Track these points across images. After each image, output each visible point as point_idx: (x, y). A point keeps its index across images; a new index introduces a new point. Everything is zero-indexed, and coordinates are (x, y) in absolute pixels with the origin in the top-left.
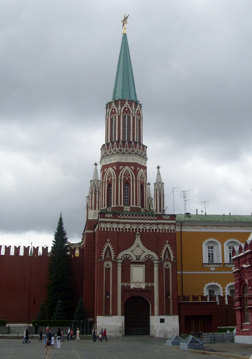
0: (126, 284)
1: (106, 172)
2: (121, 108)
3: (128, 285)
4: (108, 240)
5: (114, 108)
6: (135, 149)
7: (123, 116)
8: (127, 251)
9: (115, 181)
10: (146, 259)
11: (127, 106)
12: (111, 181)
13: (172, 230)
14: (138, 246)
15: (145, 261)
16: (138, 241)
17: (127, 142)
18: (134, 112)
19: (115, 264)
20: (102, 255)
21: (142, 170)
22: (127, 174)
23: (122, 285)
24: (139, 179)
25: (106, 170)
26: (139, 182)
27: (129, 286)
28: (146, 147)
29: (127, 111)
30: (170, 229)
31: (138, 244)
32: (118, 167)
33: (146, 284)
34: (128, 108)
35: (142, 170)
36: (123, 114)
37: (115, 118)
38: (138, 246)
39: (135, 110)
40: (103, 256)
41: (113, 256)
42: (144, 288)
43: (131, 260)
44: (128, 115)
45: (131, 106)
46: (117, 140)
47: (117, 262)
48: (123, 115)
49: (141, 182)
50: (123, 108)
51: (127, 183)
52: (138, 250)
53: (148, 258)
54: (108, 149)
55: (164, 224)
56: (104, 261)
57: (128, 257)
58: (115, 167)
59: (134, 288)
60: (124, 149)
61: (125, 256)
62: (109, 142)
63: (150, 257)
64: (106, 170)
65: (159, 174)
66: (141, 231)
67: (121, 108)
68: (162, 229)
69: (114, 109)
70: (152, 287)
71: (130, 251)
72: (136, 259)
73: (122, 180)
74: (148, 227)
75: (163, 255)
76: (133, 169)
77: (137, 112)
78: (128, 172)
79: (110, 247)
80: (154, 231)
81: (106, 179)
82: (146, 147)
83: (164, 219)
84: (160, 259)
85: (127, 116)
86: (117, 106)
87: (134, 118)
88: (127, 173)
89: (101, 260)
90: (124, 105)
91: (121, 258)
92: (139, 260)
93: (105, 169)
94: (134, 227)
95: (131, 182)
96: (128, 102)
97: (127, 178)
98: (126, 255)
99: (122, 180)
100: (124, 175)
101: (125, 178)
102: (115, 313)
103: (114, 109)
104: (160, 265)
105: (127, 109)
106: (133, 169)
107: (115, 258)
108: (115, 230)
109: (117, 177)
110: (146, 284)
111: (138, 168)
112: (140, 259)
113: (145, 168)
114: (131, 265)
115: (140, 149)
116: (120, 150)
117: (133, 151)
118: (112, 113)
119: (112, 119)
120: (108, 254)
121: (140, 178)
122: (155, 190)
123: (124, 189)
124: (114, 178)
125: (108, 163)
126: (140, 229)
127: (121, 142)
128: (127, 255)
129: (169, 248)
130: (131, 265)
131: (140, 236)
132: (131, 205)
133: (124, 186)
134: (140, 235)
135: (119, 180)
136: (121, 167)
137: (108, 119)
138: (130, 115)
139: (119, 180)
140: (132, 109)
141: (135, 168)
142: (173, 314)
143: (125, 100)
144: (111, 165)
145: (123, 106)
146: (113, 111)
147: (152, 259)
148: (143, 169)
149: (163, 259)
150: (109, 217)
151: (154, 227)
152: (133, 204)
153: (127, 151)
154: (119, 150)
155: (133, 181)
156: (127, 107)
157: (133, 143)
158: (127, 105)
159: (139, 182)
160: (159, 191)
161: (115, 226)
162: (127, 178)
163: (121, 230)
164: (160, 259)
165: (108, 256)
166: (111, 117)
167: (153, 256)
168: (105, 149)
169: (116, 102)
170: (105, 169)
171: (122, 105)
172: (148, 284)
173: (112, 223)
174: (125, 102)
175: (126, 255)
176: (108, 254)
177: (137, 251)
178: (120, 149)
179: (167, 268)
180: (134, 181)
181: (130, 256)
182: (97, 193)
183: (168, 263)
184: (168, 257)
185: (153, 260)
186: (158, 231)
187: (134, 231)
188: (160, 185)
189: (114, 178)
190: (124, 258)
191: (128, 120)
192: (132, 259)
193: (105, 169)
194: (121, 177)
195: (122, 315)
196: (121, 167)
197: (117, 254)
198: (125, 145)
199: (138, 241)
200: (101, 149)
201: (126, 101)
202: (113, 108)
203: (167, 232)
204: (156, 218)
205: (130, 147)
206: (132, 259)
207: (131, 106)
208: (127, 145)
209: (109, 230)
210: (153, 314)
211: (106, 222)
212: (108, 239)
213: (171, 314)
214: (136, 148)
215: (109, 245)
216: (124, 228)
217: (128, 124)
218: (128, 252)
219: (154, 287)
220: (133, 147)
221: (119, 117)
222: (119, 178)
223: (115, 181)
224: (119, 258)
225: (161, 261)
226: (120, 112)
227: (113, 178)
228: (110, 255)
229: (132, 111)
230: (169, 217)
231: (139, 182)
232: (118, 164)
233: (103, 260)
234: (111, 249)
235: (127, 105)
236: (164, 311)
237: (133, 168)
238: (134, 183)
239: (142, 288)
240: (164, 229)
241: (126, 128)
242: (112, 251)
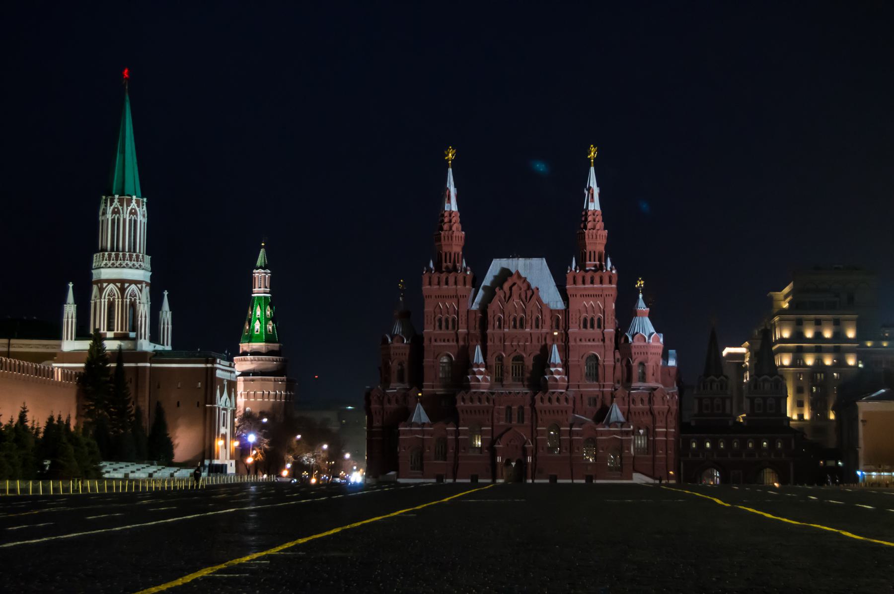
22: (133, 295)
32: (123, 285)
37: (118, 220)
45: (138, 206)
50: (129, 208)
58: (119, 285)
86: (122, 205)
93: (105, 285)
109: (122, 298)
118: (114, 212)
119: (113, 220)
136: (126, 285)
153: (134, 265)
171: (128, 205)
221: (124, 220)
232: (123, 282)
237: (139, 286)
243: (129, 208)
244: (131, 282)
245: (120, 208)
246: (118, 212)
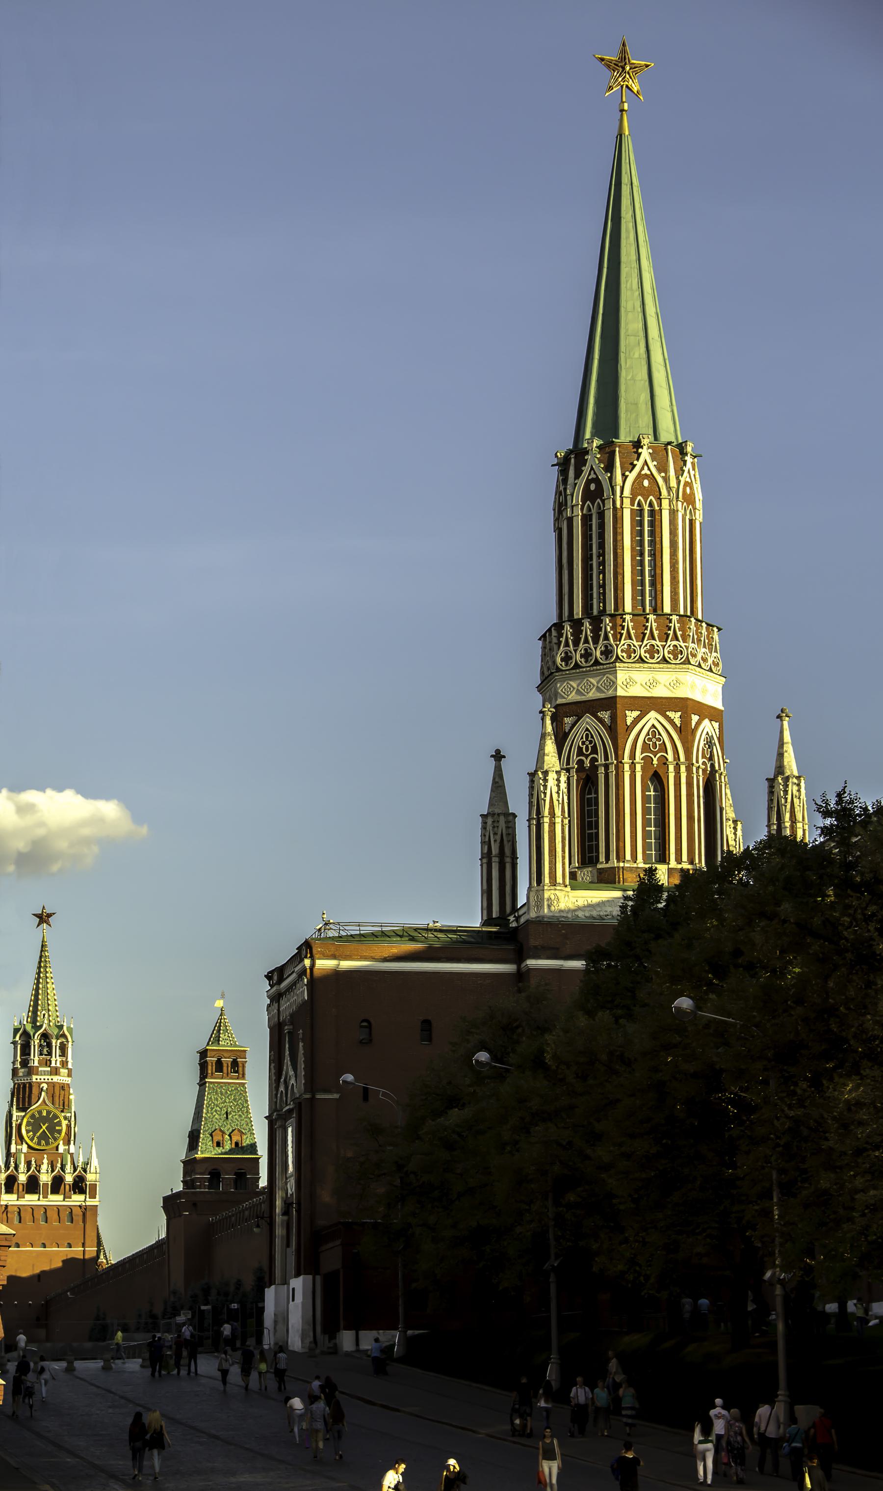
2: (625, 478)
5: (593, 476)
6: (683, 645)
9: (612, 768)
11: (646, 467)
12: (594, 768)
17: (652, 617)
24: (699, 761)
26: (697, 772)
29: (646, 489)
34: (652, 477)
37: (601, 515)
39: (679, 483)
44: (651, 505)
45: (663, 468)
46: (611, 608)
49: (704, 771)
50: (632, 476)
54: (576, 643)
62: (578, 612)
67: (625, 478)
69: (593, 480)
76: (678, 722)
77: (684, 490)
78: (660, 734)
81: (575, 758)
85: (646, 508)
87: (673, 513)
88: (654, 740)
90: (635, 462)
96: (650, 451)
99: (638, 767)
100: (645, 748)
101: (647, 761)
103: (597, 481)
105: (646, 483)
106: (678, 722)
111: (695, 718)
117: (676, 652)
121: (703, 758)
123: (646, 799)
124: (606, 758)
127: (628, 617)
132: (673, 864)
133: (645, 789)
135: (627, 767)
137: (570, 520)
139: (627, 767)
140: (666, 480)
141: (685, 719)
143: (637, 444)
146: (593, 487)
148: (711, 720)
152: (679, 860)
153: (652, 651)
154: (622, 651)
156: (649, 473)
158: (646, 463)
159: (701, 771)
162: (655, 762)
168: (563, 640)
170: (566, 720)
174: (640, 450)
180: (683, 768)
189: (606, 758)
196: (631, 715)
198: (646, 629)
200: (544, 636)
201: (642, 447)
205: (665, 638)
207: (663, 468)
208: (654, 628)
222: (626, 759)
226: (622, 493)
229: (669, 489)
231: (701, 771)
235: (646, 463)
237: (676, 716)
243: (632, 476)
244: (645, 704)
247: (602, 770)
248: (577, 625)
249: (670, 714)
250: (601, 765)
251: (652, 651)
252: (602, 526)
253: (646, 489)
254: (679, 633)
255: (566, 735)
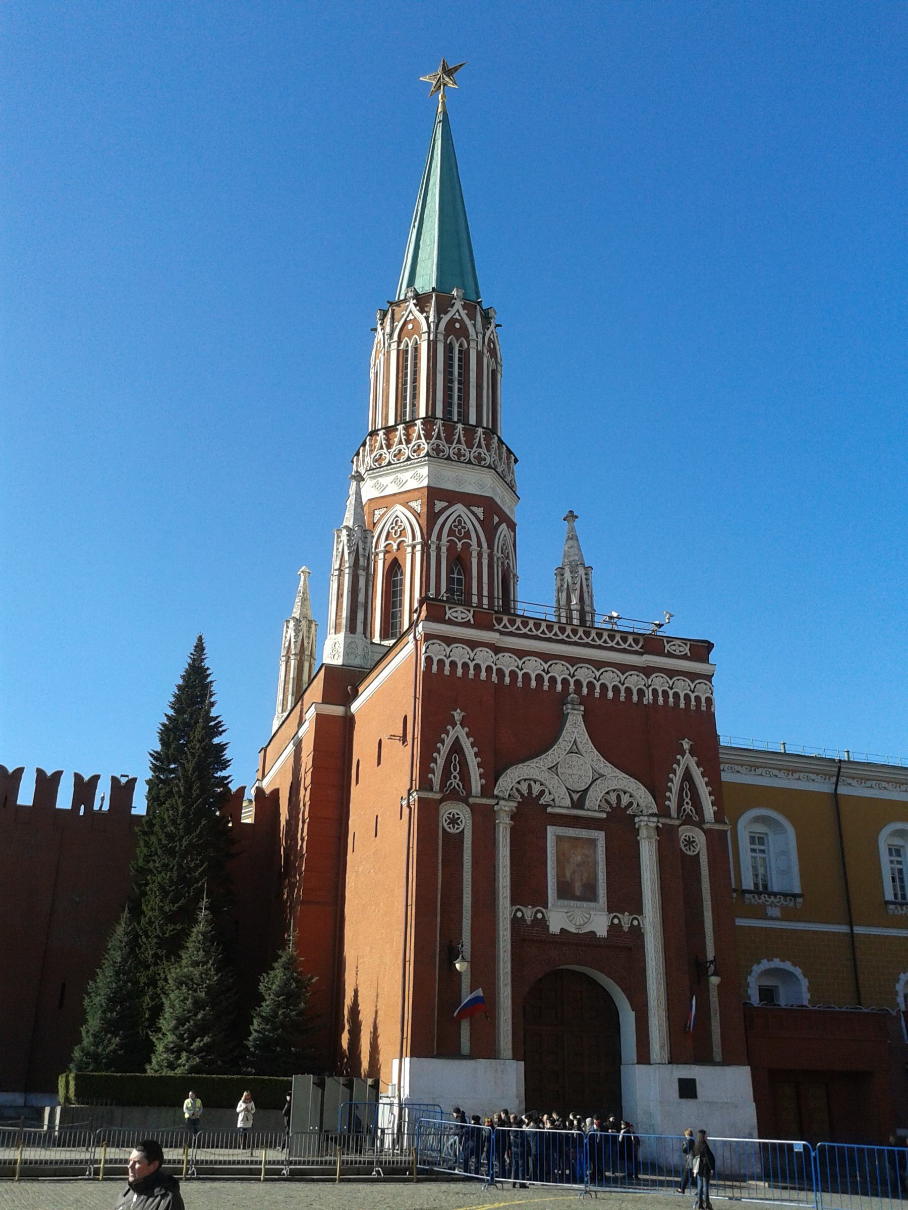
0: (528, 913)
1: (379, 520)
3: (539, 916)
4: (458, 715)
5: (411, 317)
7: (445, 343)
8: (532, 765)
10: (609, 810)
13: (703, 700)
14: (575, 750)
15: (604, 815)
16: (575, 728)
18: (480, 336)
19: (484, 819)
20: (430, 776)
21: (504, 526)
22: (458, 530)
23: (515, 914)
25: (382, 516)
27: (542, 924)
28: (516, 461)
30: (693, 696)
31: (575, 741)
32: (430, 505)
33: (612, 915)
34: (461, 321)
35: (504, 526)
36: (446, 337)
37: (416, 349)
38: (575, 750)
40: (436, 779)
41: (476, 784)
42: (602, 931)
43: (550, 805)
47: (496, 808)
48: (446, 339)
49: (503, 563)
50: (445, 319)
51: (459, 561)
52: (573, 768)
53: (614, 802)
55: (671, 673)
56: (441, 801)
57: (535, 792)
58: (417, 505)
59: (562, 929)
60: (449, 448)
61: (524, 788)
63: (625, 800)
64: (382, 516)
65: (573, 537)
66: (585, 691)
67: (440, 319)
68: (665, 693)
70: (637, 933)
71: (545, 769)
72: (568, 802)
73: (444, 549)
74: (610, 678)
75: (673, 796)
79: (466, 743)
80: (635, 698)
81: (382, 544)
82: (516, 461)
83: (670, 655)
84: (663, 812)
87: (480, 355)
88: (460, 527)
89: (430, 795)
91: (509, 795)
92: (583, 809)
94: (559, 671)
95: (473, 559)
97: (459, 545)
98: (529, 784)
99: (444, 549)
100: (451, 532)
102: (485, 1049)
104: (666, 838)
105: (457, 325)
107: (487, 791)
108: (483, 675)
110: (613, 918)
112: (587, 804)
113: (512, 526)
114: (550, 830)
115: (500, 458)
116: (437, 450)
117: (480, 458)
119: (402, 355)
120: (455, 774)
122: (559, 590)
123: (450, 580)
124: (414, 538)
125: (392, 489)
126: (578, 683)
128: (532, 783)
129: (696, 772)
130: (550, 830)
131: (582, 708)
133: (450, 571)
134: (581, 704)
135: (433, 547)
137: (389, 352)
138: (469, 345)
140: (474, 325)
142: (728, 1061)
144: (403, 498)
145: (446, 313)
147: (629, 812)
149: (674, 813)
150: (459, 620)
151: (635, 681)
153: (459, 454)
155: (480, 555)
157: (480, 431)
158: (458, 311)
160: (578, 592)
161: (484, 657)
162: (459, 545)
163: (507, 680)
164: (663, 812)
165: (455, 782)
166: (398, 346)
167: (638, 797)
169: (421, 301)
172: (619, 915)
173: (473, 645)
175: (530, 786)
176: (455, 774)
177: (571, 772)
178: (438, 445)
179: (690, 853)
180: (485, 556)
181: (543, 788)
182: (361, 572)
183: (690, 834)
184: (690, 807)
185: (635, 816)
186: (651, 697)
187: (559, 687)
188: (581, 571)
189: (414, 538)
190: (522, 795)
191: (460, 360)
192: (552, 803)
193: (377, 512)
194: (439, 538)
195: (515, 1057)
196: (439, 505)
197: (492, 775)
199: (575, 728)
202: (408, 316)
203: (682, 706)
204: (636, 648)
205: (470, 445)
206: (552, 803)
209: (460, 672)
210: (644, 1057)
211: (449, 641)
212: (458, 710)
213: (718, 1057)
214: (488, 447)
215: (459, 732)
216: (520, 674)
217: (460, 374)
218: (531, 770)
219: (643, 934)
220: (479, 446)
223: (419, 547)
224: (501, 794)
225: (668, 821)
227: (409, 540)
228: (465, 776)
230: (686, 650)
233: (438, 796)
234: (470, 753)
235: (458, 311)
236: (690, 1046)
237: (479, 511)
238: (485, 562)
239: (593, 933)
240: (671, 693)
241: (456, 386)
242: (473, 762)
243: (445, 319)
244: (452, 497)
245: (421, 318)
246: (417, 328)
247: (409, 549)
248: (389, 430)
249: (474, 509)
250: (408, 546)
251: (459, 454)
252: (416, 358)
253: (455, 330)
254: (483, 443)
255: (374, 524)
